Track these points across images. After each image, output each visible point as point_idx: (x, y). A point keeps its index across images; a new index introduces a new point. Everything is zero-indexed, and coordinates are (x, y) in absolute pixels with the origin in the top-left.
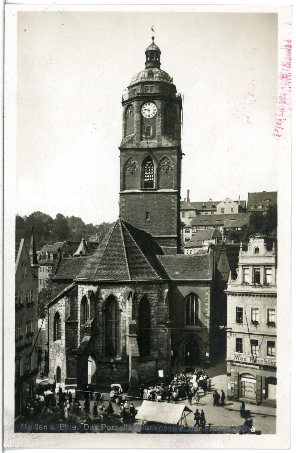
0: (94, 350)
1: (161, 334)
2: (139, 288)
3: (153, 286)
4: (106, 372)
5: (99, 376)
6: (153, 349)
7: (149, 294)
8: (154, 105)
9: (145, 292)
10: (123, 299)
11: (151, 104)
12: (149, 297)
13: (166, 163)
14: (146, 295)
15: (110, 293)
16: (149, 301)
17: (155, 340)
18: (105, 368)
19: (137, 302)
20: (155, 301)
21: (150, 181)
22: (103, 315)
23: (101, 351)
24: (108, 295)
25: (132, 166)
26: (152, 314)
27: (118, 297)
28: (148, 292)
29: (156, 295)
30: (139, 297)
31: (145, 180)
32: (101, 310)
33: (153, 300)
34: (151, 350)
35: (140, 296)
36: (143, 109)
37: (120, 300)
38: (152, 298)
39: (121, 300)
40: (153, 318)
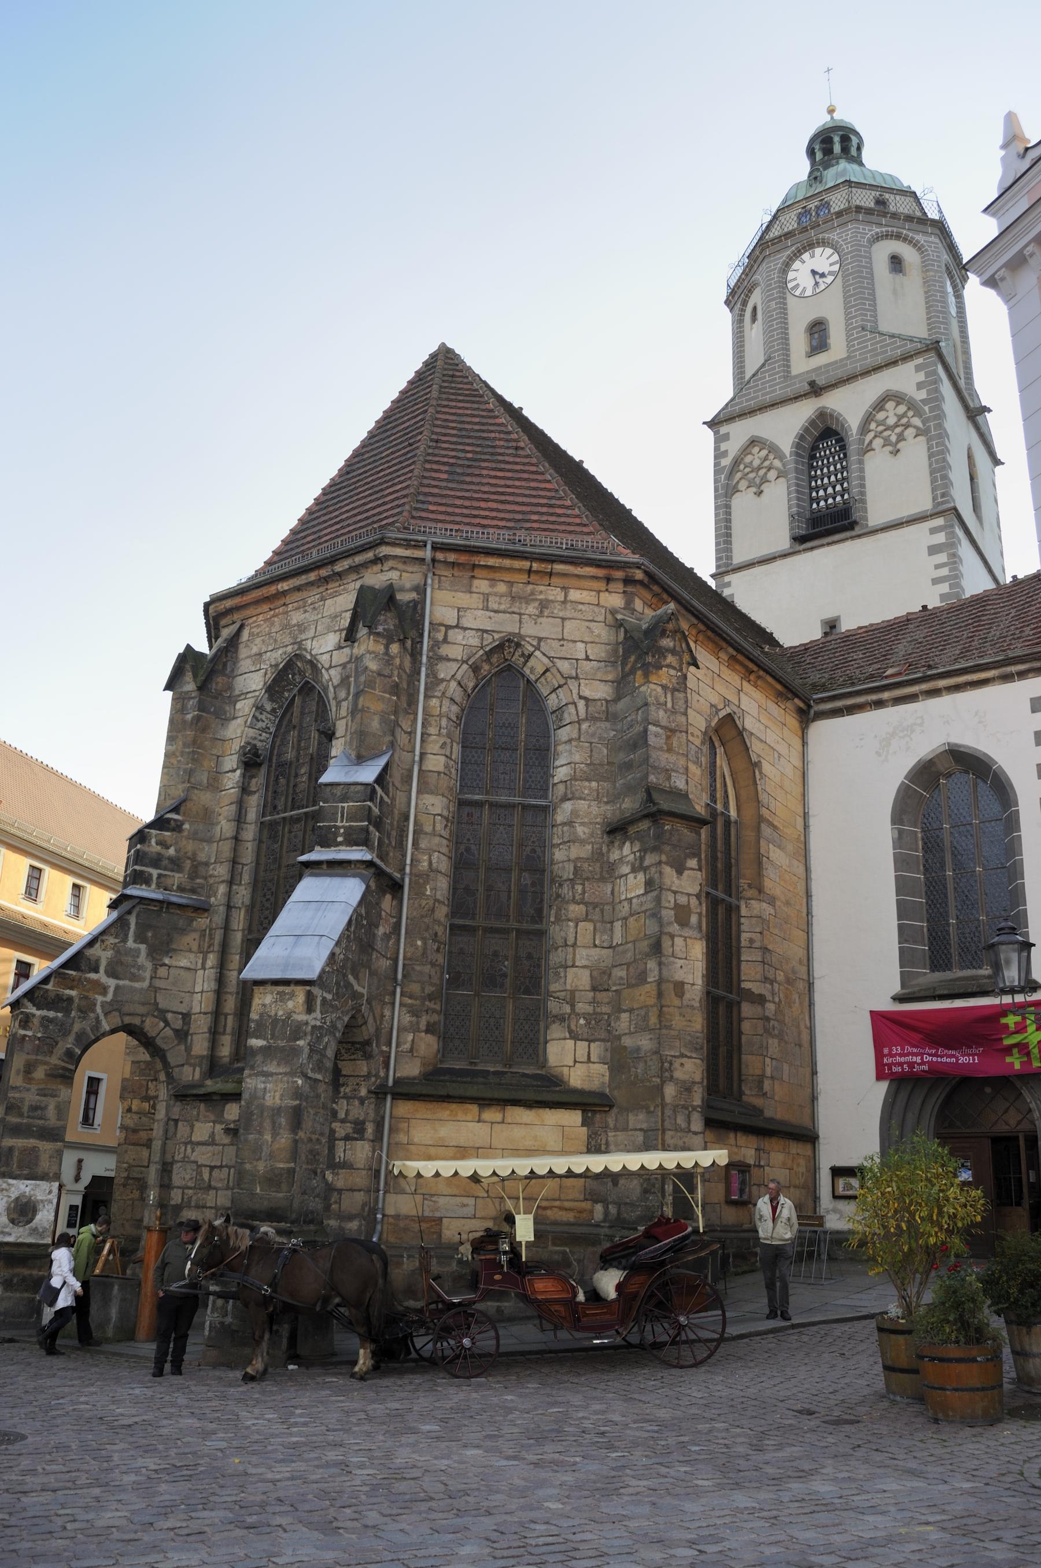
0: (162, 1014)
1: (625, 909)
2: (463, 599)
3: (574, 595)
4: (212, 1168)
5: (176, 1197)
6: (561, 1019)
7: (540, 639)
8: (829, 251)
9: (508, 625)
10: (344, 666)
11: (818, 251)
12: (538, 663)
13: (892, 421)
14: (509, 644)
15: (289, 649)
16: (545, 692)
17: (583, 956)
18: (212, 1142)
19: (434, 681)
20: (587, 692)
21: (835, 505)
22: (245, 790)
23: (201, 1025)
24: (277, 665)
25: (759, 468)
26: (561, 773)
27: (324, 659)
28: (529, 629)
29: (597, 652)
30: (453, 651)
31: (815, 506)
32: (235, 758)
33: (573, 684)
34: (556, 1031)
35: (461, 645)
36: (791, 275)
37: (332, 672)
38: (565, 666)
39: (335, 675)
40: (565, 798)
